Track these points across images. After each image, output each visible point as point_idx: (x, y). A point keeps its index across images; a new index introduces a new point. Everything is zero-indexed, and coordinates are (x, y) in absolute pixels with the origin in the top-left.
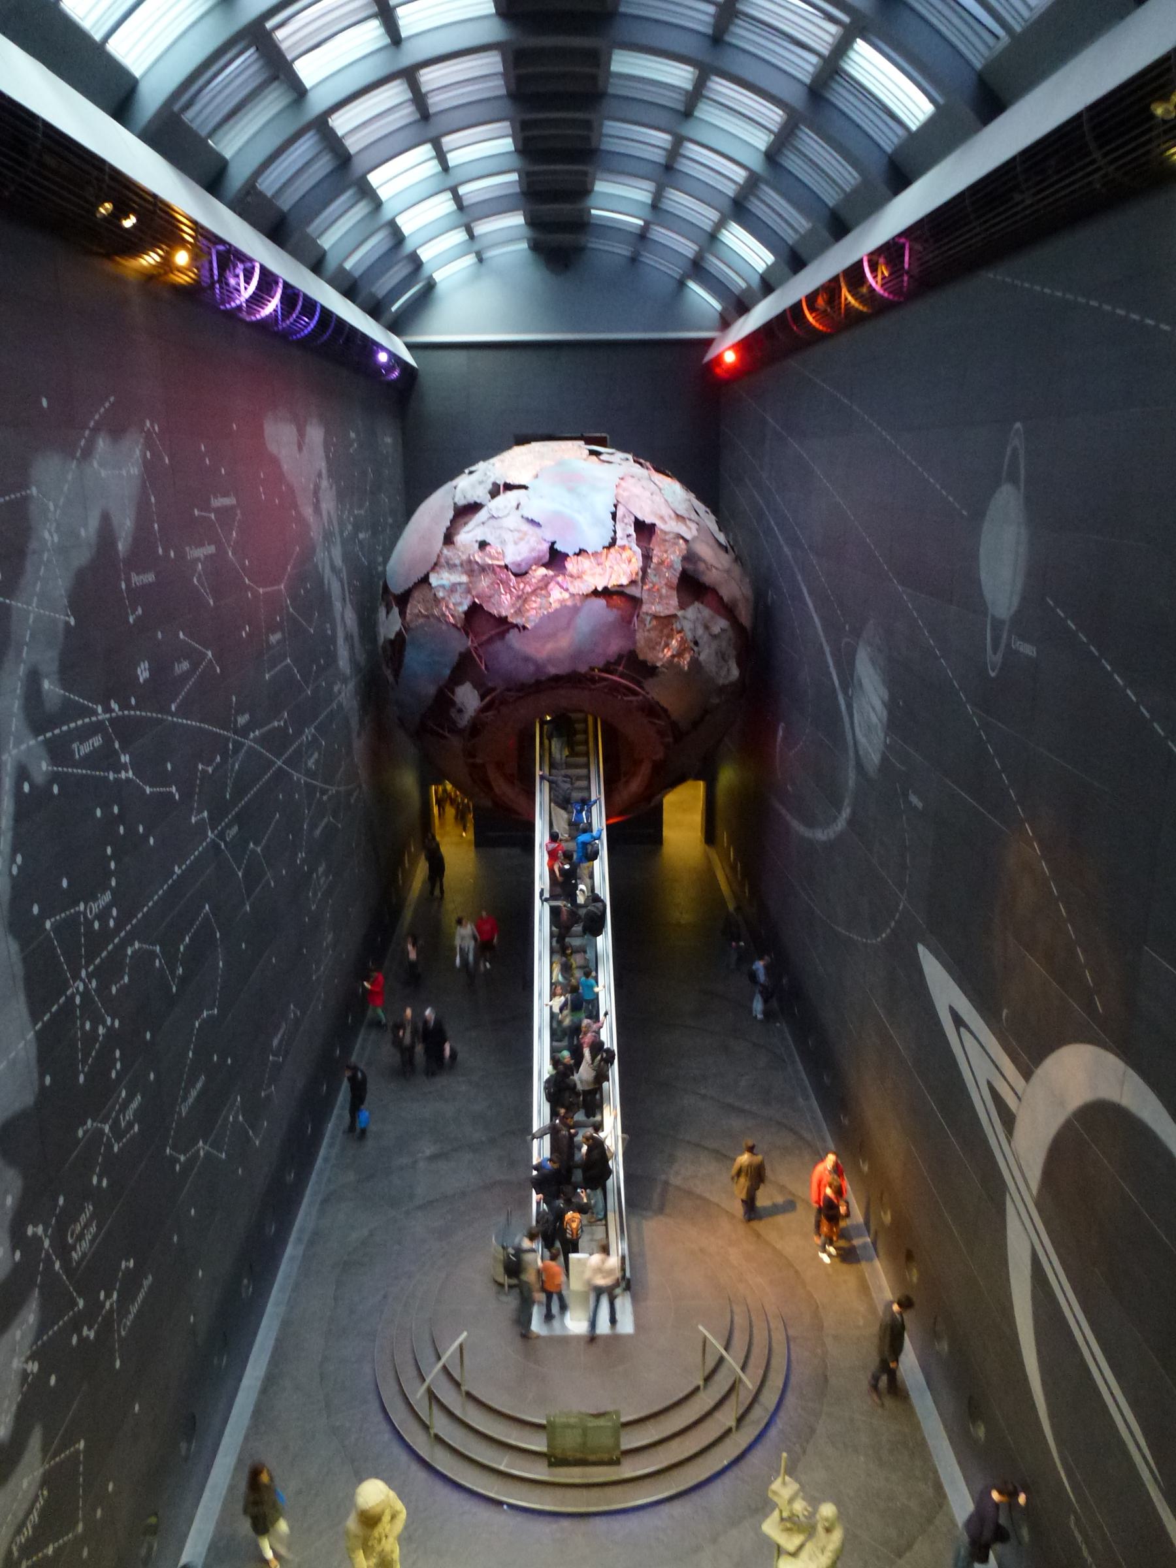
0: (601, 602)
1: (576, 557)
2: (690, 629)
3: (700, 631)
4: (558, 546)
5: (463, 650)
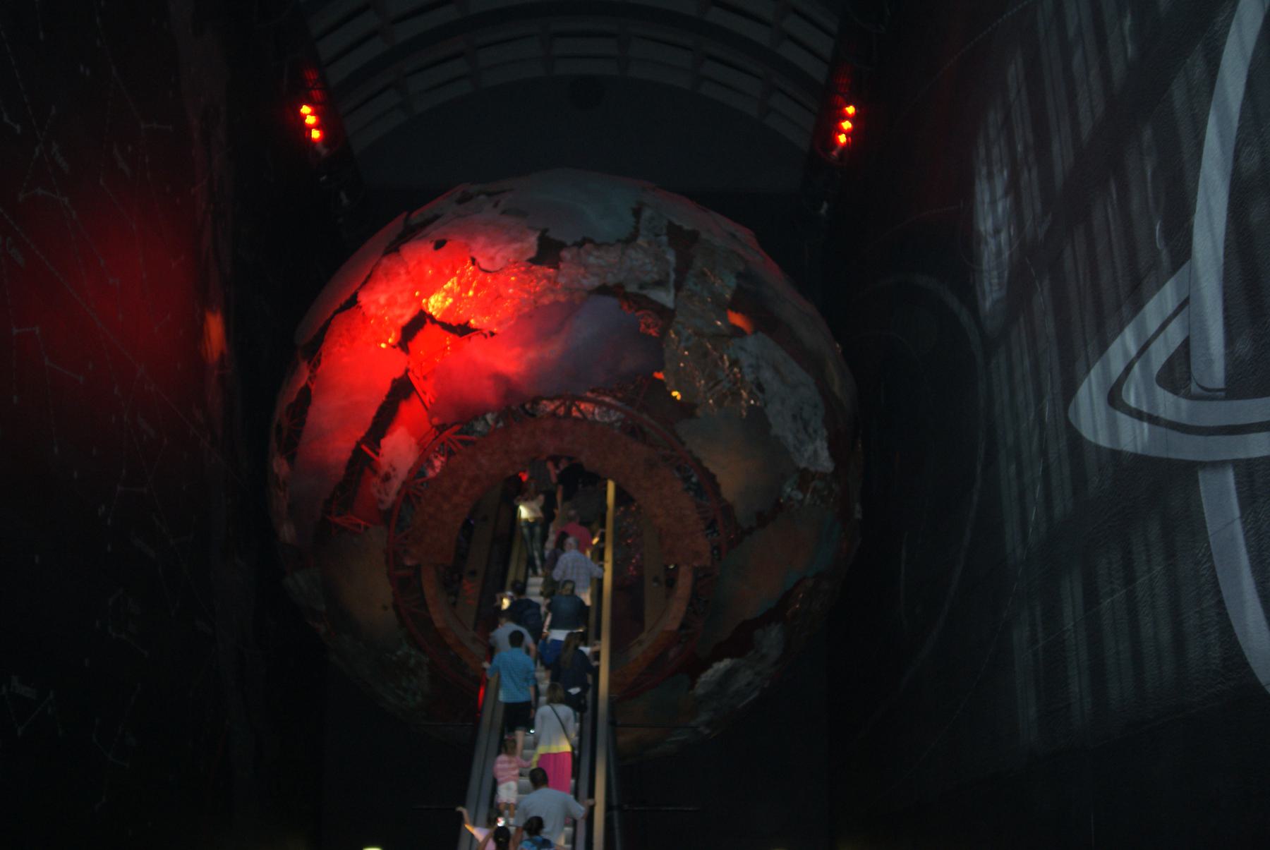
0: (611, 302)
1: (575, 250)
2: (751, 366)
3: (767, 375)
4: (553, 234)
5: (398, 374)
